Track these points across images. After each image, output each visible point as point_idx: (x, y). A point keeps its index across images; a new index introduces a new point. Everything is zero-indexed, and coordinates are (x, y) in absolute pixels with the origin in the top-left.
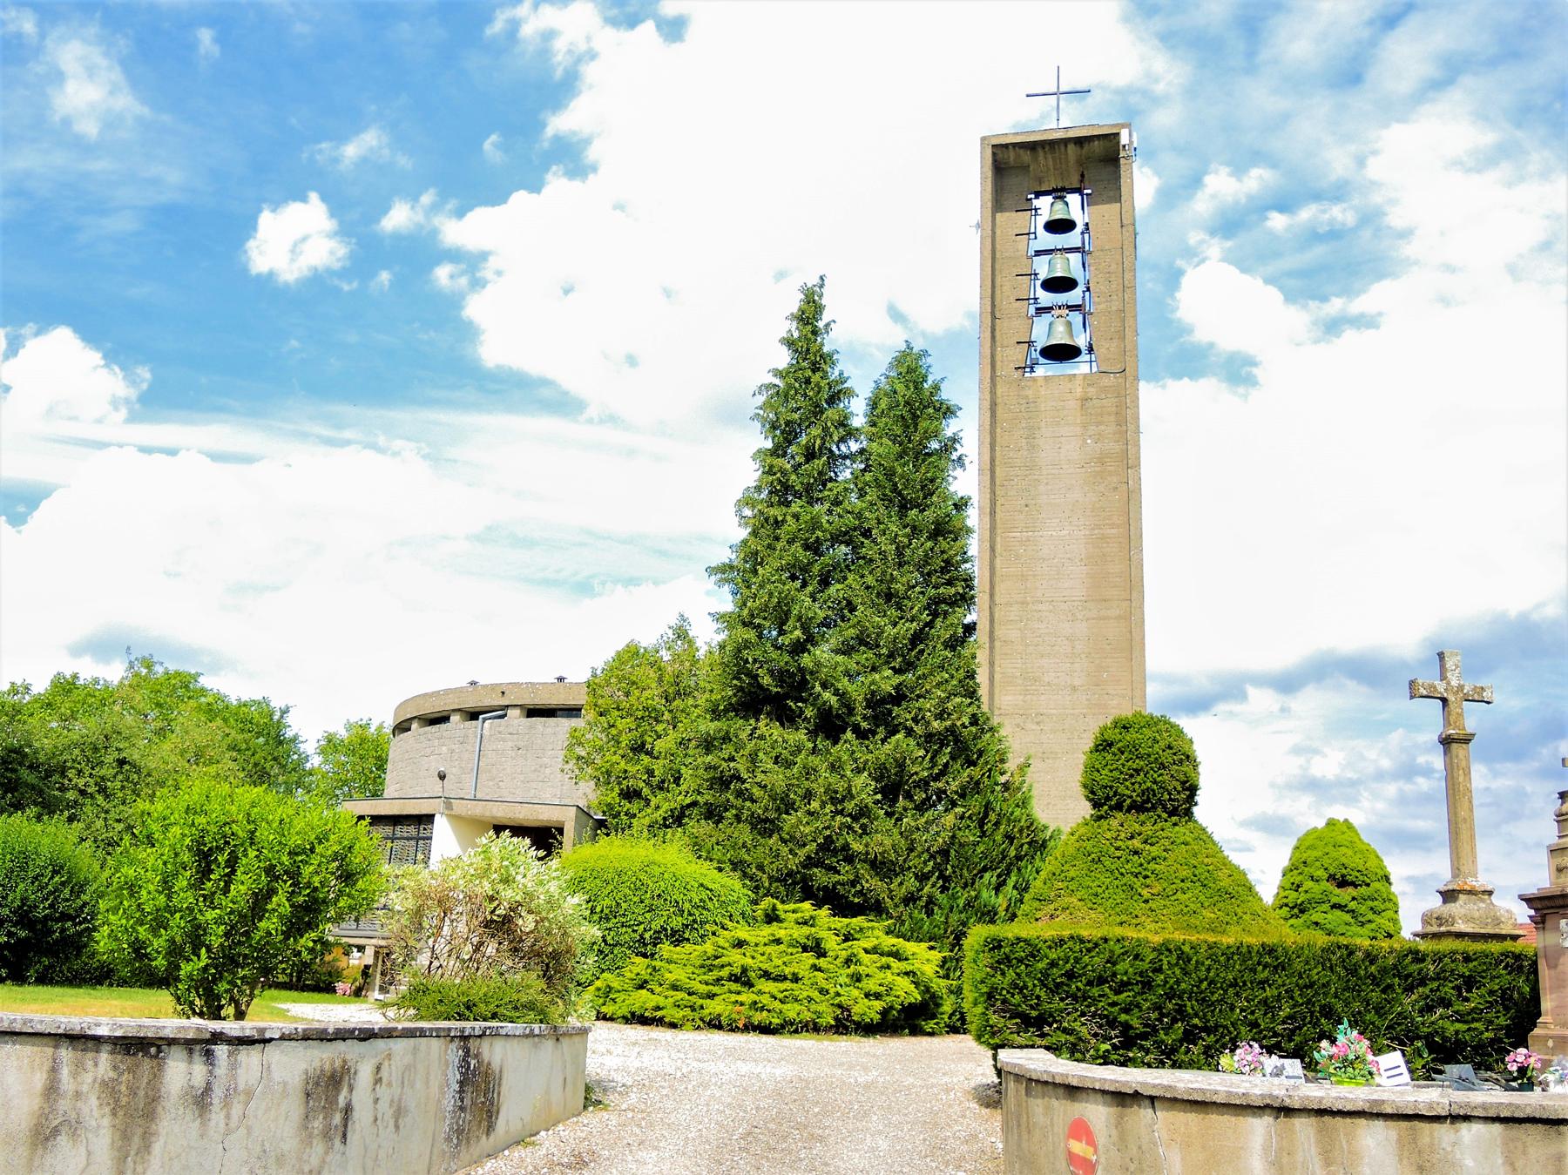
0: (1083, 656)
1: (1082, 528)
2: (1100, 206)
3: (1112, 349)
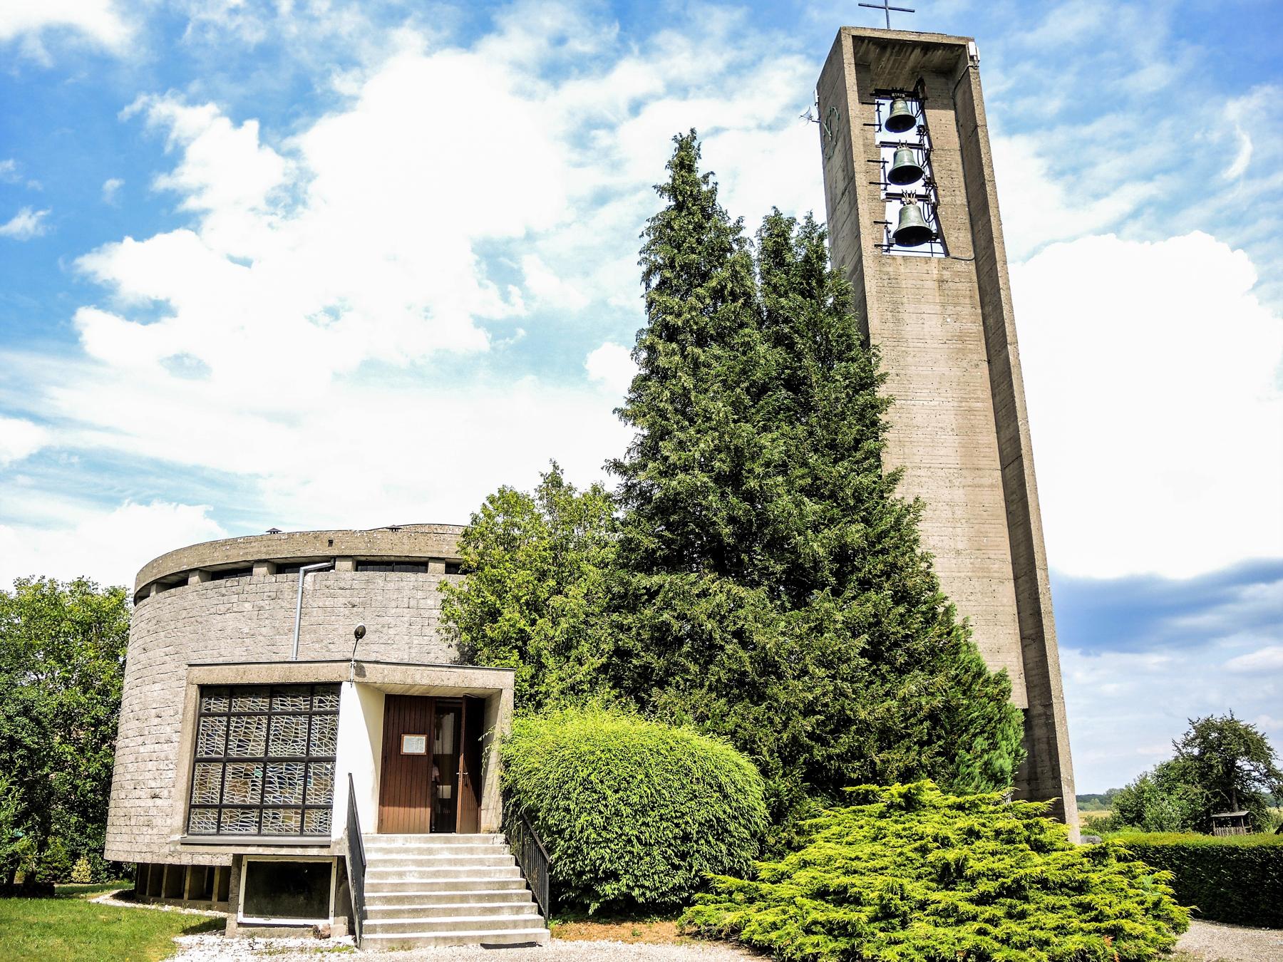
0: (963, 521)
1: (950, 400)
2: (937, 111)
3: (960, 239)
